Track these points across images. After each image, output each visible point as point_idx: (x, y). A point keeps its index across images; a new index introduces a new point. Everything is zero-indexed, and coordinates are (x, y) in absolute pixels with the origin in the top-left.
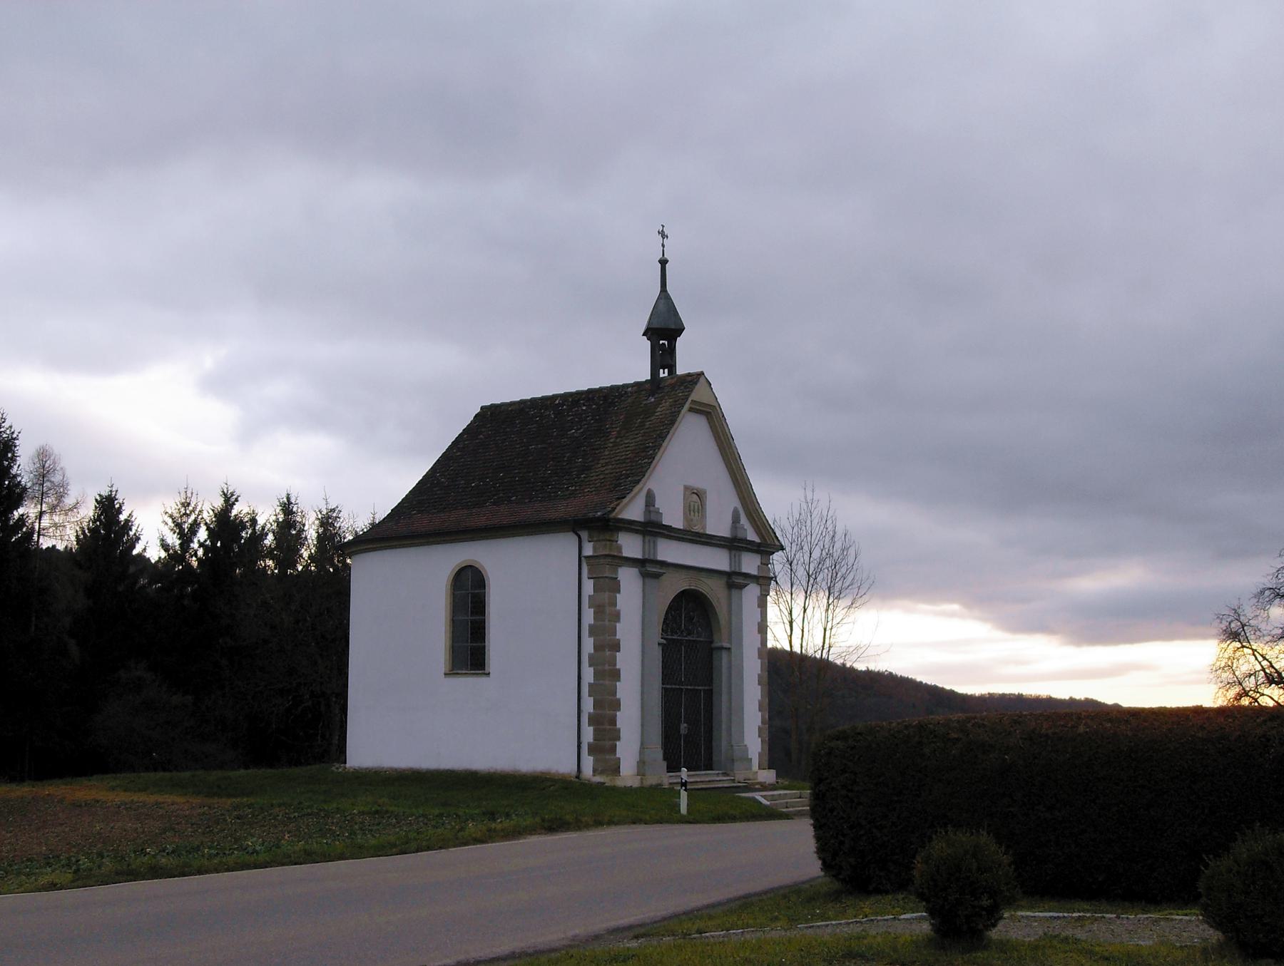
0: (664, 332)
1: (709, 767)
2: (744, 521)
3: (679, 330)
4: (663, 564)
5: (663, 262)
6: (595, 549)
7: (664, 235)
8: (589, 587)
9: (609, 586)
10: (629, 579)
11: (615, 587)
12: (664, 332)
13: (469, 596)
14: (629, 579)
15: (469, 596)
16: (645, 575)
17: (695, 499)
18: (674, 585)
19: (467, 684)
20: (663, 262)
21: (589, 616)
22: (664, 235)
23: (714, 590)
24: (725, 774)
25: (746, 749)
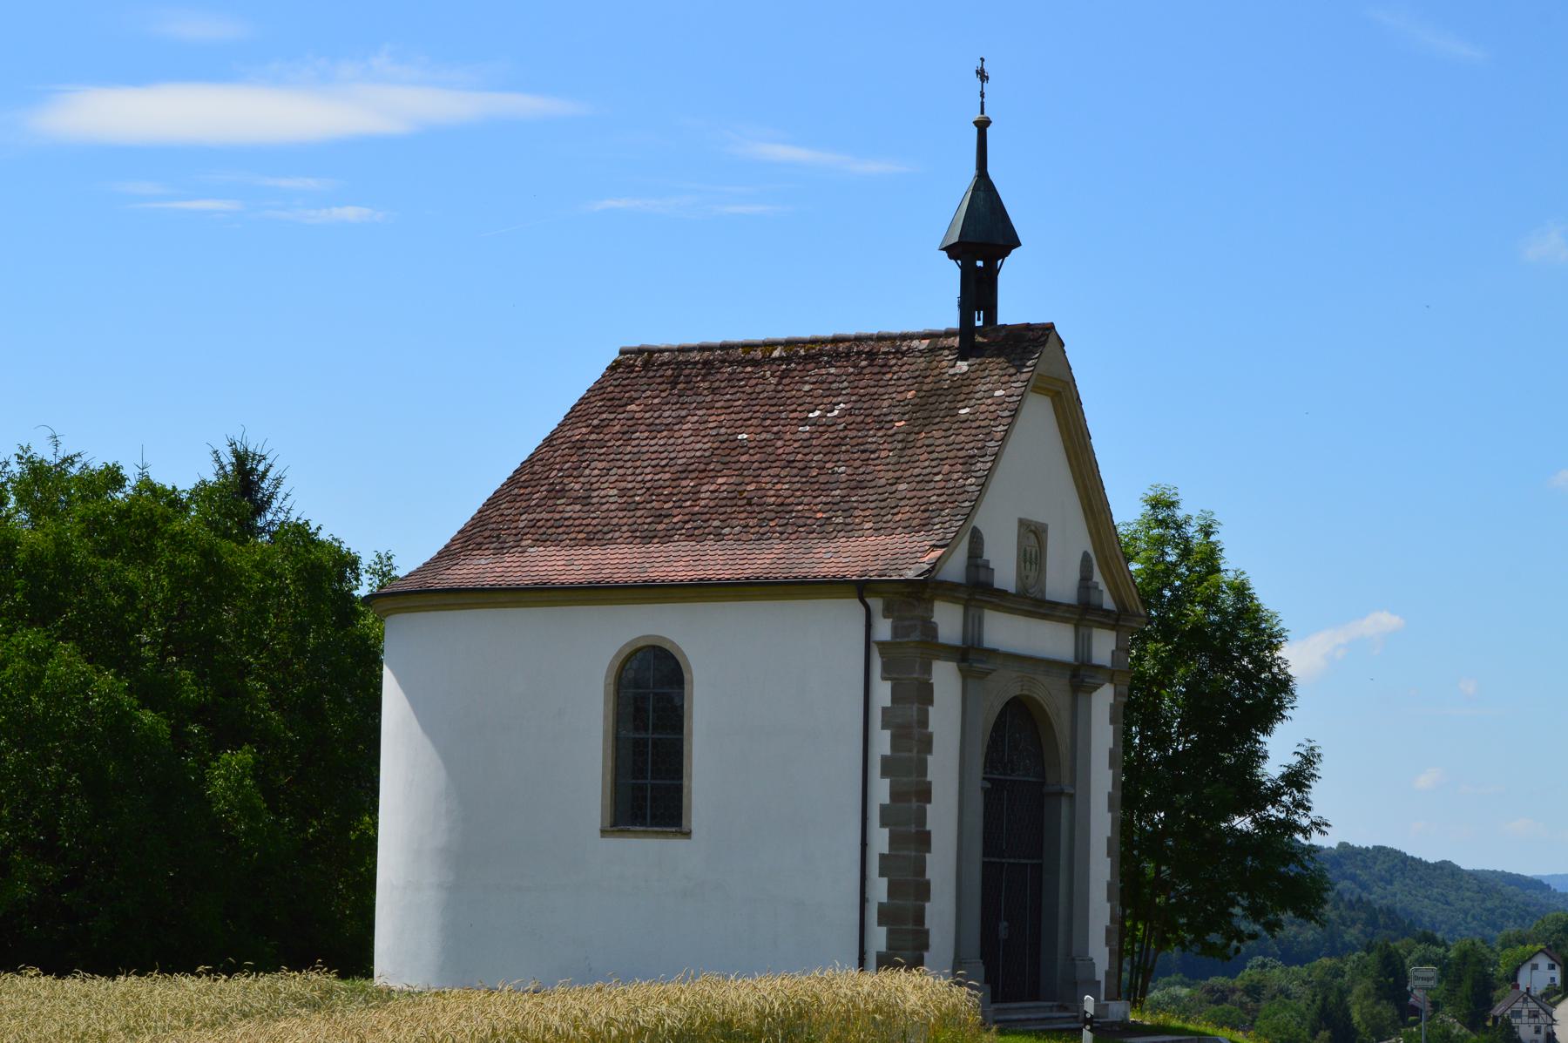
0: (983, 240)
1: (1035, 996)
2: (1097, 577)
3: (1010, 241)
4: (993, 652)
5: (982, 126)
6: (896, 630)
7: (982, 75)
8: (883, 693)
9: (915, 693)
10: (945, 678)
11: (925, 694)
12: (983, 240)
13: (650, 706)
14: (945, 678)
15: (650, 706)
16: (966, 675)
17: (1033, 536)
18: (1005, 686)
19: (644, 851)
20: (982, 126)
21: (882, 742)
22: (982, 75)
23: (1052, 695)
24: (1063, 1008)
25: (1091, 964)
